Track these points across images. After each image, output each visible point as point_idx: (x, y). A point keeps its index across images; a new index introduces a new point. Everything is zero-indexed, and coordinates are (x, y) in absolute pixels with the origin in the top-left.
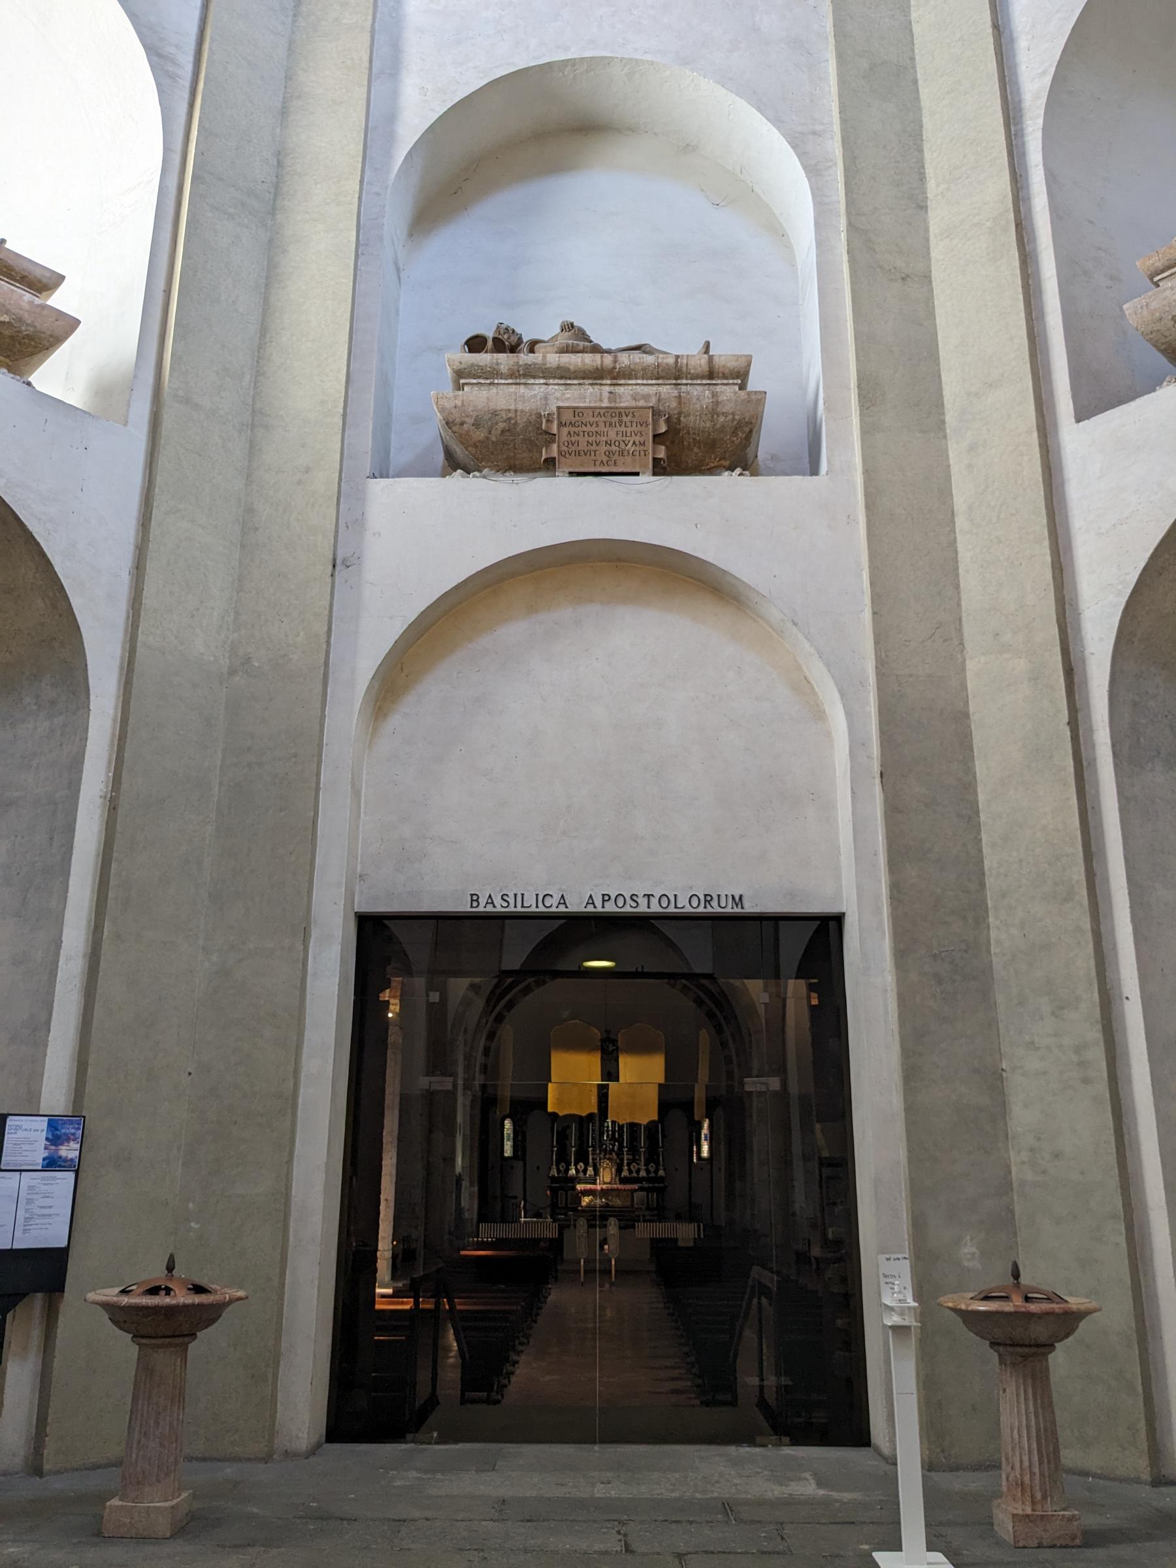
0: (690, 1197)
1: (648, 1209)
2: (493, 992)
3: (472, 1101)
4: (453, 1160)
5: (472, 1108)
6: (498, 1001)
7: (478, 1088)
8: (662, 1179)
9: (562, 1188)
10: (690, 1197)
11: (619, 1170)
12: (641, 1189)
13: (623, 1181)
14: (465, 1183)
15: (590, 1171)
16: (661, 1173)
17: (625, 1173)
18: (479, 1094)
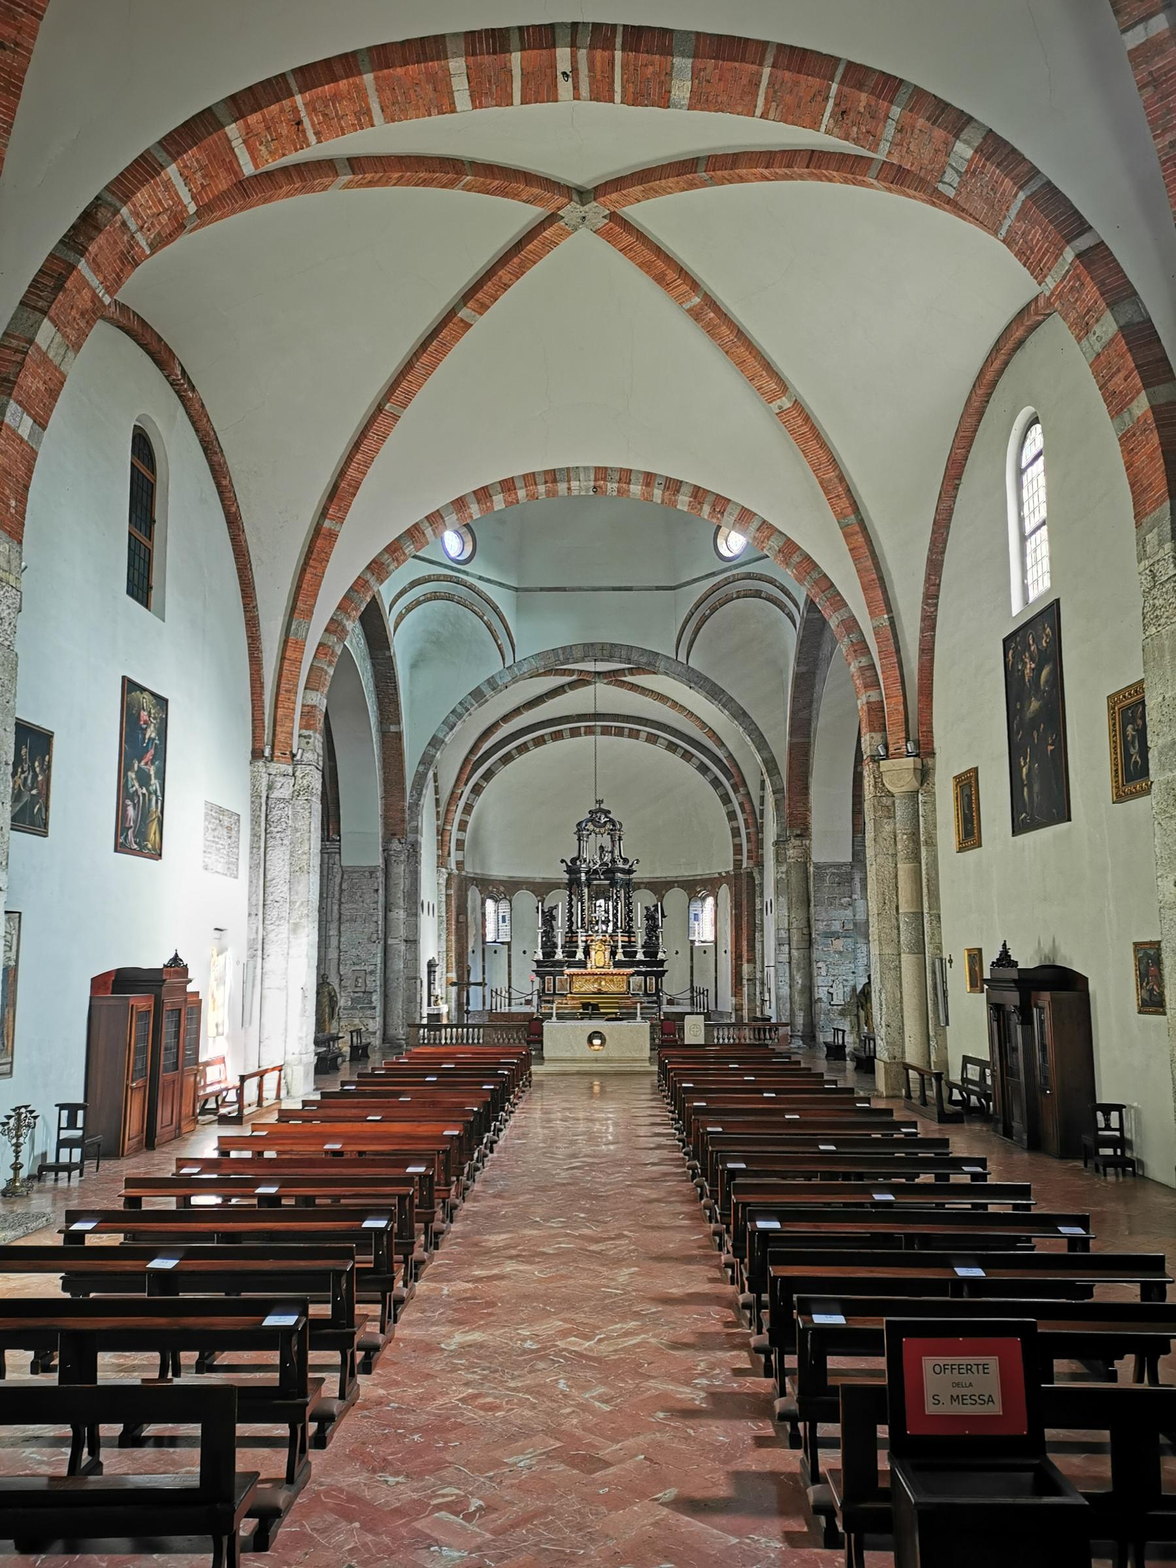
0: (692, 981)
1: (646, 994)
2: (467, 759)
3: (448, 880)
4: (413, 942)
5: (448, 886)
6: (474, 770)
7: (453, 866)
8: (662, 962)
9: (550, 973)
10: (692, 981)
11: (613, 954)
12: (638, 973)
13: (618, 964)
14: (440, 970)
15: (580, 955)
16: (661, 956)
17: (620, 956)
18: (455, 872)
